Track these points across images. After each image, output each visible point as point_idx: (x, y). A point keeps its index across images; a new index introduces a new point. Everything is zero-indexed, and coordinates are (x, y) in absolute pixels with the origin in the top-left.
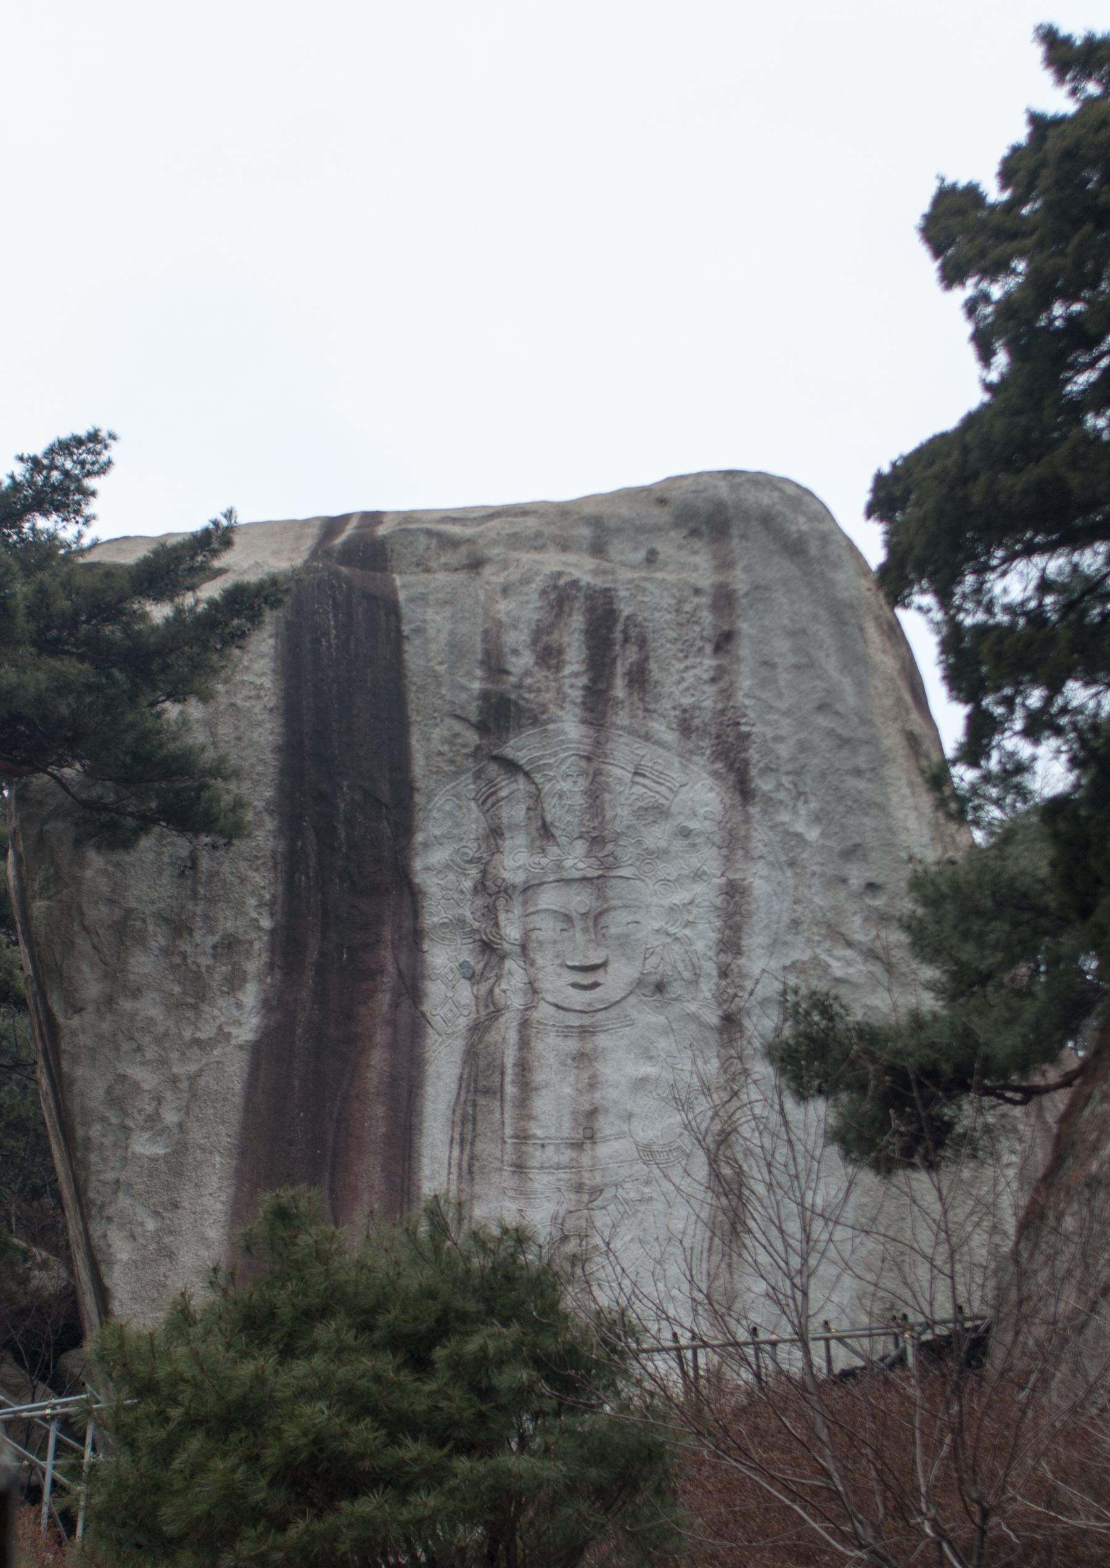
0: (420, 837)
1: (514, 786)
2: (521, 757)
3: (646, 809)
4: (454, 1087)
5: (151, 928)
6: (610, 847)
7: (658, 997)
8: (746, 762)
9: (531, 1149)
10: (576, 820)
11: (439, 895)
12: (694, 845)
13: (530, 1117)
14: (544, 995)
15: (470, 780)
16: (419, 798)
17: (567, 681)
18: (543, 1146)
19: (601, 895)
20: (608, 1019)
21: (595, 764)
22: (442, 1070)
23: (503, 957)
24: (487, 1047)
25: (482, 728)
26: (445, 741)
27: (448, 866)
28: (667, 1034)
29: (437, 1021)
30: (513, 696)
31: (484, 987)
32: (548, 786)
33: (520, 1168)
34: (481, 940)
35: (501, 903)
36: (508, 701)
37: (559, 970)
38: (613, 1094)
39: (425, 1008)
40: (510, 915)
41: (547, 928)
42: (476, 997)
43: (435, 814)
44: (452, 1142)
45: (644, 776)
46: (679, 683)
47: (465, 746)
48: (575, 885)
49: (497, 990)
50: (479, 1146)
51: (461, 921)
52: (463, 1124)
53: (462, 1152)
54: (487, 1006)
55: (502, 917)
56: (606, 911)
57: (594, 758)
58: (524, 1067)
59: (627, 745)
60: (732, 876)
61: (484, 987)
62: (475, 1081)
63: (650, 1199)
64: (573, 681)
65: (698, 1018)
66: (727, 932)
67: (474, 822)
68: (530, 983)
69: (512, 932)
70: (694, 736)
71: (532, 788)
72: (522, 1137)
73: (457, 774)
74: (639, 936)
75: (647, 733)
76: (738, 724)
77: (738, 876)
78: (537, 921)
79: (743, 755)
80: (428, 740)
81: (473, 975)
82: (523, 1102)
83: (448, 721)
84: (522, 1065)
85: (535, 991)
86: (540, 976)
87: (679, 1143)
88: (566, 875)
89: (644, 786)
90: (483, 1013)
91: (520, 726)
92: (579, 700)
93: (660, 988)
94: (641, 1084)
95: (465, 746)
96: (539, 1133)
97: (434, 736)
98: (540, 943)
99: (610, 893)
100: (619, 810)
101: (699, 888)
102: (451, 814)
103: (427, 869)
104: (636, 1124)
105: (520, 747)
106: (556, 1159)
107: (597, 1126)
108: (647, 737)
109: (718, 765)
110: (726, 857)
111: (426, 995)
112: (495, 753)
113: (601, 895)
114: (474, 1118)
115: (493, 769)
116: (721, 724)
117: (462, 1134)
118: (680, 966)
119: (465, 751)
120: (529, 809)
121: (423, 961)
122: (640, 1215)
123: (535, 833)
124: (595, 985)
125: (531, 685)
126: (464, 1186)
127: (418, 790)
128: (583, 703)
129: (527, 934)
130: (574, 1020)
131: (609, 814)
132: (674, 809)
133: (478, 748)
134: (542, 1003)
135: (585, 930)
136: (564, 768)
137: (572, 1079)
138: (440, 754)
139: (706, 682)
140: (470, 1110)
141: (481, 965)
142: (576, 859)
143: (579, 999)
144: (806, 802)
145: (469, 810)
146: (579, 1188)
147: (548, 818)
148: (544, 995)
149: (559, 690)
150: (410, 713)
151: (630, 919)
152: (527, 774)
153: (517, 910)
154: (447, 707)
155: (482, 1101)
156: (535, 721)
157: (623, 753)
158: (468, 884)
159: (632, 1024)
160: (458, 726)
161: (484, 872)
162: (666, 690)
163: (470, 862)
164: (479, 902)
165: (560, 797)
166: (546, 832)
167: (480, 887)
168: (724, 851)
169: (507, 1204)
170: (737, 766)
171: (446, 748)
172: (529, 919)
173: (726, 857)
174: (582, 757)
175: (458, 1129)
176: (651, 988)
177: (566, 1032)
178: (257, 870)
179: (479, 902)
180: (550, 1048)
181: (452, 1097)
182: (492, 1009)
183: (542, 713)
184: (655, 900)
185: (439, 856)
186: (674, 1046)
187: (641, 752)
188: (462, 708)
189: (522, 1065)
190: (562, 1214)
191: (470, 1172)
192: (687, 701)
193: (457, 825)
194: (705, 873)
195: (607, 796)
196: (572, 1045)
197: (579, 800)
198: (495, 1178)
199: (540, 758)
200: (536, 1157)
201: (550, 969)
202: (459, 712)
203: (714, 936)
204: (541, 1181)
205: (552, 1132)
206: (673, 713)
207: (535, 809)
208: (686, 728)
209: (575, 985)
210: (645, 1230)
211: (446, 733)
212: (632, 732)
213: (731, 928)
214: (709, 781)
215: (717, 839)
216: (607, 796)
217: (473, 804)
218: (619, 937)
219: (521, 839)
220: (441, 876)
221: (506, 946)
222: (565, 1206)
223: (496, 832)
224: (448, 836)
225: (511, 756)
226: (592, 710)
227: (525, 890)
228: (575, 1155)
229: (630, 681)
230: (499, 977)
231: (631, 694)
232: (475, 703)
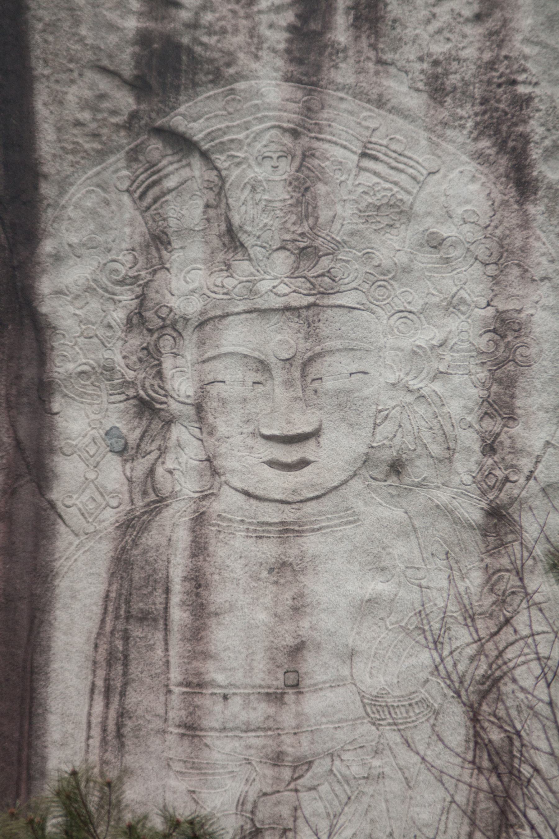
0: (48, 246)
1: (185, 173)
2: (197, 130)
3: (378, 208)
4: (97, 610)
6: (325, 263)
7: (393, 480)
8: (525, 139)
9: (207, 702)
10: (277, 224)
12: (447, 261)
13: (206, 655)
14: (228, 477)
15: (122, 163)
16: (47, 189)
17: (265, 19)
18: (225, 697)
19: (311, 331)
20: (320, 513)
21: (304, 141)
22: (78, 586)
23: (169, 423)
24: (145, 552)
25: (139, 86)
26: (85, 105)
27: (89, 289)
28: (407, 535)
29: (72, 515)
30: (185, 40)
31: (141, 466)
32: (235, 173)
33: (191, 729)
35: (167, 343)
36: (178, 47)
37: (250, 441)
38: (327, 622)
39: (56, 495)
40: (180, 361)
41: (233, 380)
42: (130, 480)
43: (70, 212)
44: (92, 691)
45: (376, 159)
46: (428, 21)
47: (114, 113)
48: (275, 318)
49: (160, 471)
50: (132, 698)
51: (109, 370)
52: (109, 665)
53: (107, 706)
54: (145, 493)
55: (168, 363)
56: (319, 355)
57: (304, 129)
58: (197, 582)
59: (351, 113)
60: (501, 307)
61: (141, 466)
62: (128, 602)
63: (381, 776)
64: (273, 17)
65: (451, 512)
66: (495, 388)
67: (127, 225)
68: (208, 460)
69: (181, 385)
70: (449, 100)
71: (212, 175)
72: (196, 685)
73: (102, 154)
74: (367, 392)
75: (380, 95)
76: (514, 82)
77: (511, 306)
78: (218, 370)
79: (521, 129)
80: (61, 103)
81: (125, 448)
82: (196, 633)
83: (90, 75)
84: (196, 579)
85: (215, 472)
86: (222, 450)
87: (423, 693)
88: (261, 303)
89: (376, 174)
90: (139, 503)
91: (195, 85)
92: (282, 46)
93: (396, 467)
94: (368, 607)
95: (114, 113)
96: (220, 678)
97: (70, 97)
98: (223, 402)
99: (325, 330)
100: (339, 208)
101: (454, 324)
102: (94, 213)
103: (59, 293)
104: (361, 668)
105: (196, 116)
106: (244, 716)
107: (304, 668)
108: (380, 102)
109: (484, 143)
110: (494, 277)
111: (56, 476)
113: (311, 331)
114: (126, 657)
115: (155, 147)
116: (489, 82)
117: (107, 680)
118: (427, 437)
119: (115, 120)
120: (207, 206)
121: (52, 427)
122: (366, 800)
123: (216, 242)
124: (303, 463)
125: (211, 24)
126: (109, 756)
127: (45, 177)
128: (288, 51)
129: (203, 388)
130: (272, 514)
131: (324, 214)
132: (419, 208)
133: (134, 116)
134: (225, 488)
135: (289, 383)
136: (258, 146)
137: (268, 600)
138: (78, 124)
139: (467, 20)
140: (119, 644)
141: (138, 433)
142: (275, 279)
143: (278, 483)
145: (120, 206)
146: (277, 759)
147: (236, 220)
148: (228, 477)
149: (252, 32)
150: (34, 62)
151: (354, 368)
152: (205, 156)
153: (190, 353)
154: (89, 55)
155: (137, 632)
156: (217, 78)
157: (345, 122)
158: (118, 316)
159: (355, 520)
160: (104, 84)
161: (142, 298)
162: (410, 32)
163: (122, 282)
164: (135, 341)
165: (254, 189)
166: (232, 239)
167: (137, 320)
168: (491, 270)
169: (173, 782)
170: (511, 144)
171: (86, 116)
172: (207, 367)
173: (494, 277)
174: (285, 130)
175: (101, 673)
176: (384, 468)
177: (260, 531)
179: (135, 341)
180: (237, 556)
181: (93, 625)
182: (153, 497)
183: (228, 65)
185: (76, 274)
186: (416, 551)
187: (372, 124)
188: (110, 57)
189: (196, 579)
190: (251, 798)
191: (119, 735)
192: (439, 49)
193: (103, 228)
194: (463, 301)
195: (321, 189)
196: (269, 550)
197: (281, 194)
198: (155, 743)
200: (215, 713)
201: (237, 439)
202: (105, 62)
203: (476, 393)
204: (222, 750)
205: (239, 677)
206: (418, 66)
207: (217, 207)
208: (437, 88)
209: (272, 464)
210: (372, 821)
211: (87, 94)
212: (359, 94)
213: (500, 382)
214: (471, 167)
215: (481, 251)
216: (321, 189)
217: (126, 198)
218: (337, 393)
219: (196, 250)
220: (78, 303)
221: (174, 406)
222: (257, 786)
223: (159, 240)
224: (90, 245)
225: (182, 129)
226: (300, 61)
227: (201, 325)
228: (271, 710)
229: (356, 18)
230: (162, 451)
231: (357, 38)
232: (130, 50)
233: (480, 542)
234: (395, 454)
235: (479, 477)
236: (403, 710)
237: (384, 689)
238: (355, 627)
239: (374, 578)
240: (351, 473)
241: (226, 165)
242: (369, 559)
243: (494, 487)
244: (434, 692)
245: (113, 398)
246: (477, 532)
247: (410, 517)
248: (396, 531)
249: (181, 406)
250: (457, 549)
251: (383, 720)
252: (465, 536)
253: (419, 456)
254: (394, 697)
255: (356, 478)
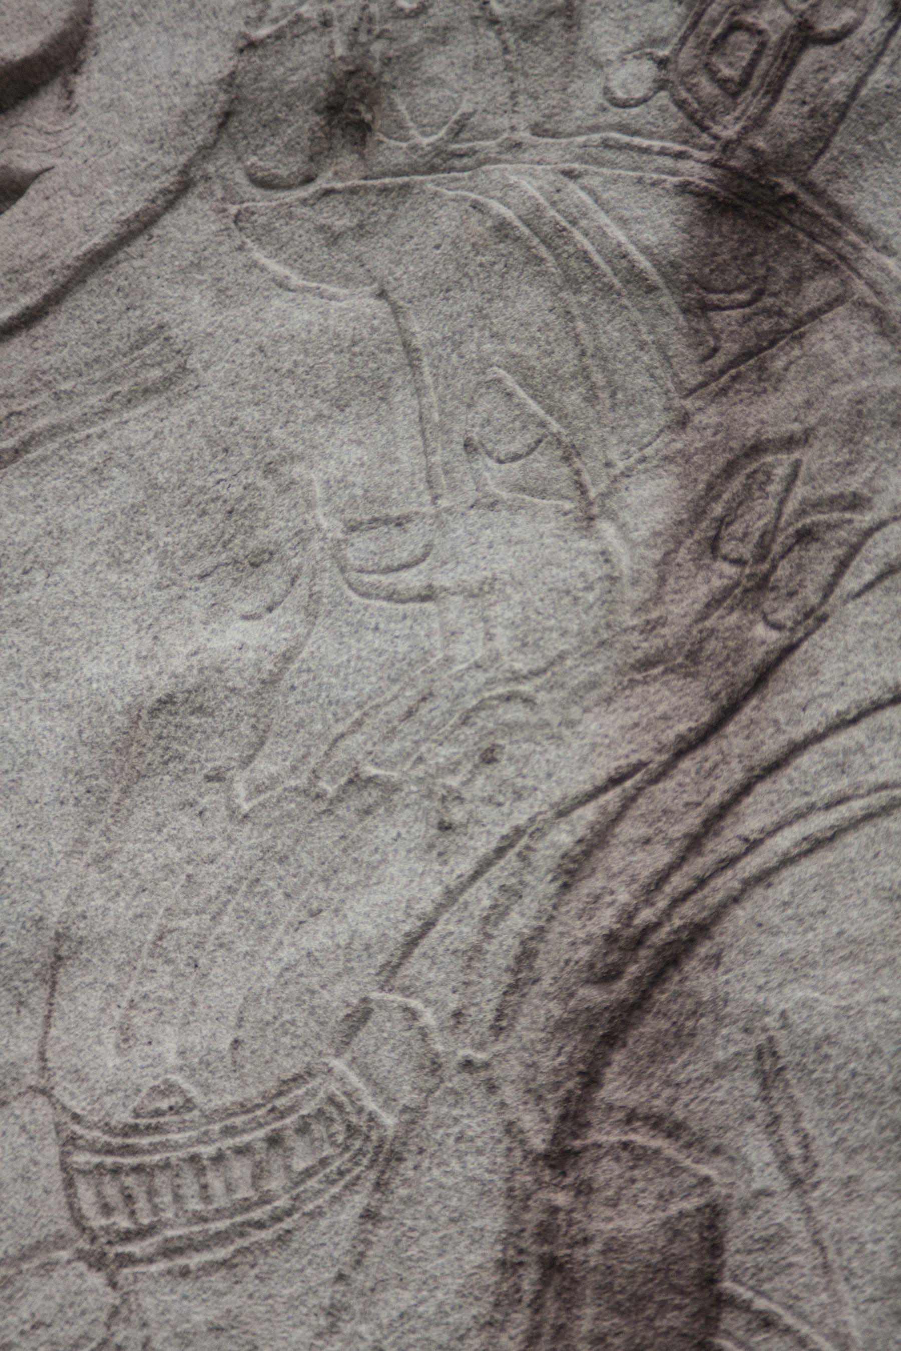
7: (342, 170)
28: (380, 390)
65: (553, 240)
176: (304, 122)
233: (678, 346)
234: (340, 50)
235: (686, 58)
236: (240, 1169)
237: (169, 1089)
238: (94, 834)
239: (217, 608)
240: (168, 181)
242: (205, 527)
243: (744, 83)
244: (385, 1060)
246: (666, 299)
247: (396, 310)
248: (330, 381)
250: (573, 399)
251: (142, 1233)
252: (611, 332)
254: (210, 1118)
255: (191, 200)
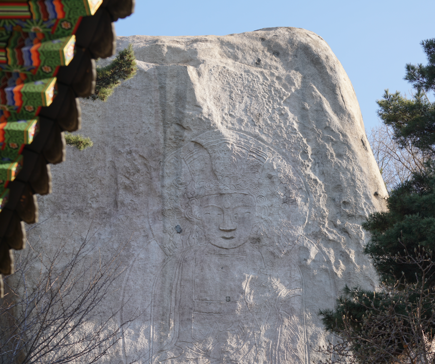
5: (46, 205)
11: (168, 197)
34: (185, 217)
49: (191, 238)
112: (193, 140)
124: (232, 238)
138: (170, 139)
144: (319, 166)
145: (181, 163)
158: (179, 193)
178: (91, 183)
184: (257, 204)
188: (180, 121)
199: (212, 143)
202: (179, 122)
221: (195, 220)
241: (212, 152)
245: (178, 217)
249: (197, 220)
253: (265, 237)
